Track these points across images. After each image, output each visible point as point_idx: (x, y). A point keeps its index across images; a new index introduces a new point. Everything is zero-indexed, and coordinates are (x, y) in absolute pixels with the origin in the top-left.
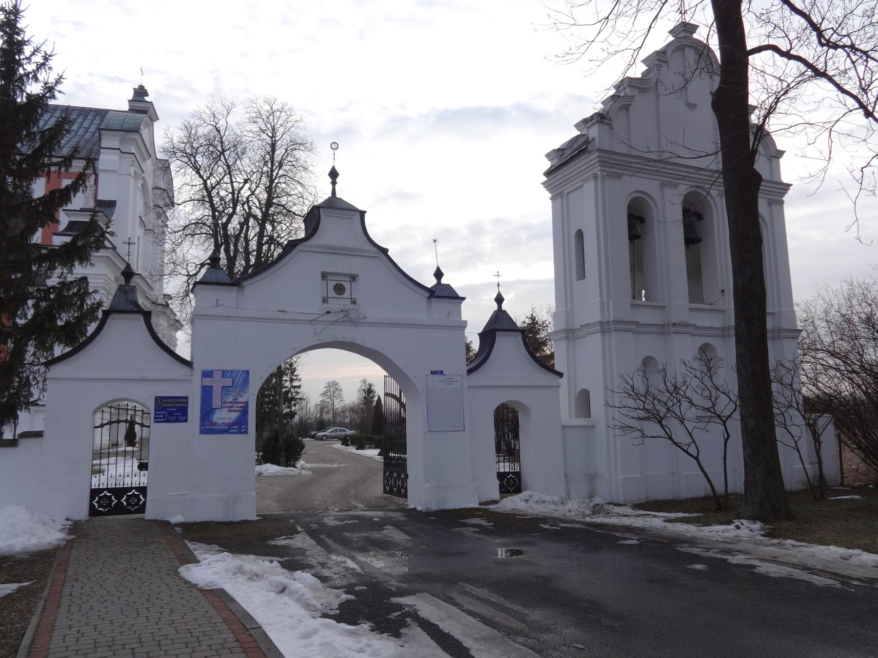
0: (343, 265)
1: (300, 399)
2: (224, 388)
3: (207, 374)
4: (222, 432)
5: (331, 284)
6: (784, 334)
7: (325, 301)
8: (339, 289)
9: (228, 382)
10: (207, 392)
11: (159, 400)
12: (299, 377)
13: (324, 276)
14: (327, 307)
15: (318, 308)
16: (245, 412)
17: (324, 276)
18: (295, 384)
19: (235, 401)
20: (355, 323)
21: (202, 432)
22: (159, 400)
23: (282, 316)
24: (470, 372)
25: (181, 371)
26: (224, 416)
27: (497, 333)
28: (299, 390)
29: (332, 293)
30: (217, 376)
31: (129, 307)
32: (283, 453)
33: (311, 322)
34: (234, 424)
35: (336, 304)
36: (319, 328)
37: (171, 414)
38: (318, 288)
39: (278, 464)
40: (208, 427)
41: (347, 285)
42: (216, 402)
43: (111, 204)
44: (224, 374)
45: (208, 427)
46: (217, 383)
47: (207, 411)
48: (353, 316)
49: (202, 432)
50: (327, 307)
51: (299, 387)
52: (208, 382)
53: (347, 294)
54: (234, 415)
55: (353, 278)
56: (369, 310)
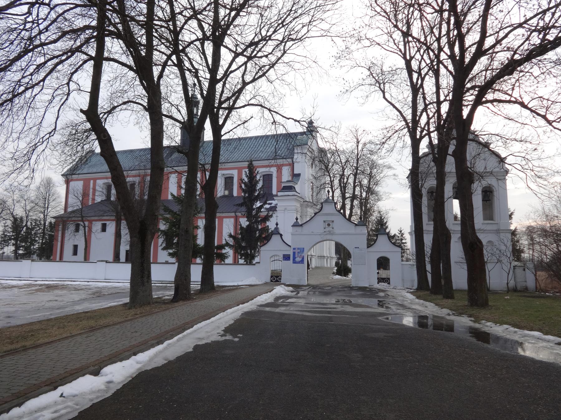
0: (329, 218)
1: (407, 249)
2: (298, 252)
3: (294, 249)
4: (297, 263)
5: (327, 224)
6: (500, 231)
7: (325, 228)
8: (329, 225)
9: (299, 251)
10: (294, 253)
11: (284, 255)
12: (405, 238)
13: (324, 221)
14: (325, 230)
15: (322, 230)
16: (303, 258)
17: (324, 221)
18: (403, 241)
19: (301, 256)
20: (332, 234)
21: (293, 263)
22: (284, 255)
23: (312, 233)
24: (368, 247)
25: (288, 248)
26: (298, 259)
27: (379, 235)
28: (406, 245)
29: (327, 226)
30: (297, 249)
31: (277, 233)
32: (343, 272)
33: (320, 235)
34: (300, 261)
35: (328, 229)
36: (322, 236)
37: (286, 258)
38: (322, 225)
39: (341, 276)
40: (294, 262)
41: (331, 224)
42: (296, 256)
43: (299, 175)
44: (298, 249)
45: (294, 262)
46: (296, 251)
47: (294, 258)
48: (332, 232)
49: (293, 263)
50: (325, 230)
51: (406, 243)
52: (294, 251)
53: (331, 226)
54: (301, 259)
55: (333, 221)
56: (336, 231)
